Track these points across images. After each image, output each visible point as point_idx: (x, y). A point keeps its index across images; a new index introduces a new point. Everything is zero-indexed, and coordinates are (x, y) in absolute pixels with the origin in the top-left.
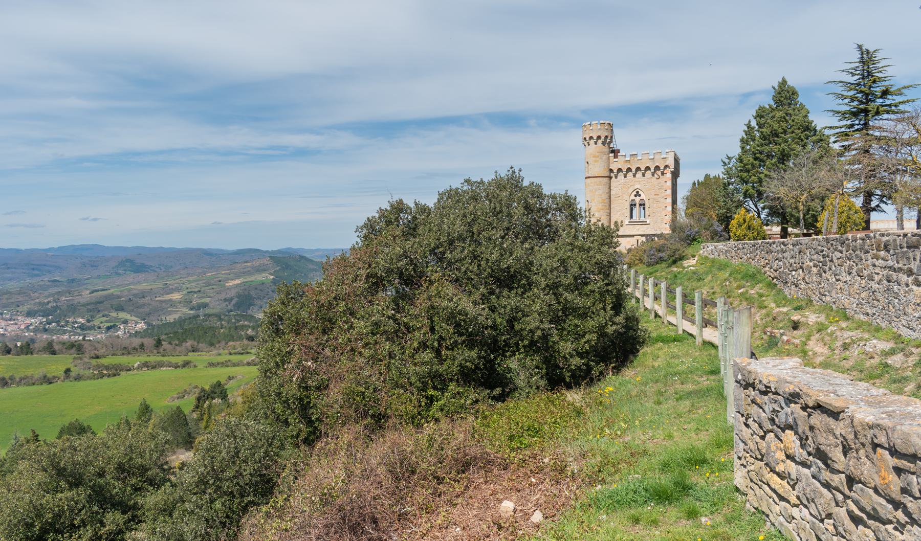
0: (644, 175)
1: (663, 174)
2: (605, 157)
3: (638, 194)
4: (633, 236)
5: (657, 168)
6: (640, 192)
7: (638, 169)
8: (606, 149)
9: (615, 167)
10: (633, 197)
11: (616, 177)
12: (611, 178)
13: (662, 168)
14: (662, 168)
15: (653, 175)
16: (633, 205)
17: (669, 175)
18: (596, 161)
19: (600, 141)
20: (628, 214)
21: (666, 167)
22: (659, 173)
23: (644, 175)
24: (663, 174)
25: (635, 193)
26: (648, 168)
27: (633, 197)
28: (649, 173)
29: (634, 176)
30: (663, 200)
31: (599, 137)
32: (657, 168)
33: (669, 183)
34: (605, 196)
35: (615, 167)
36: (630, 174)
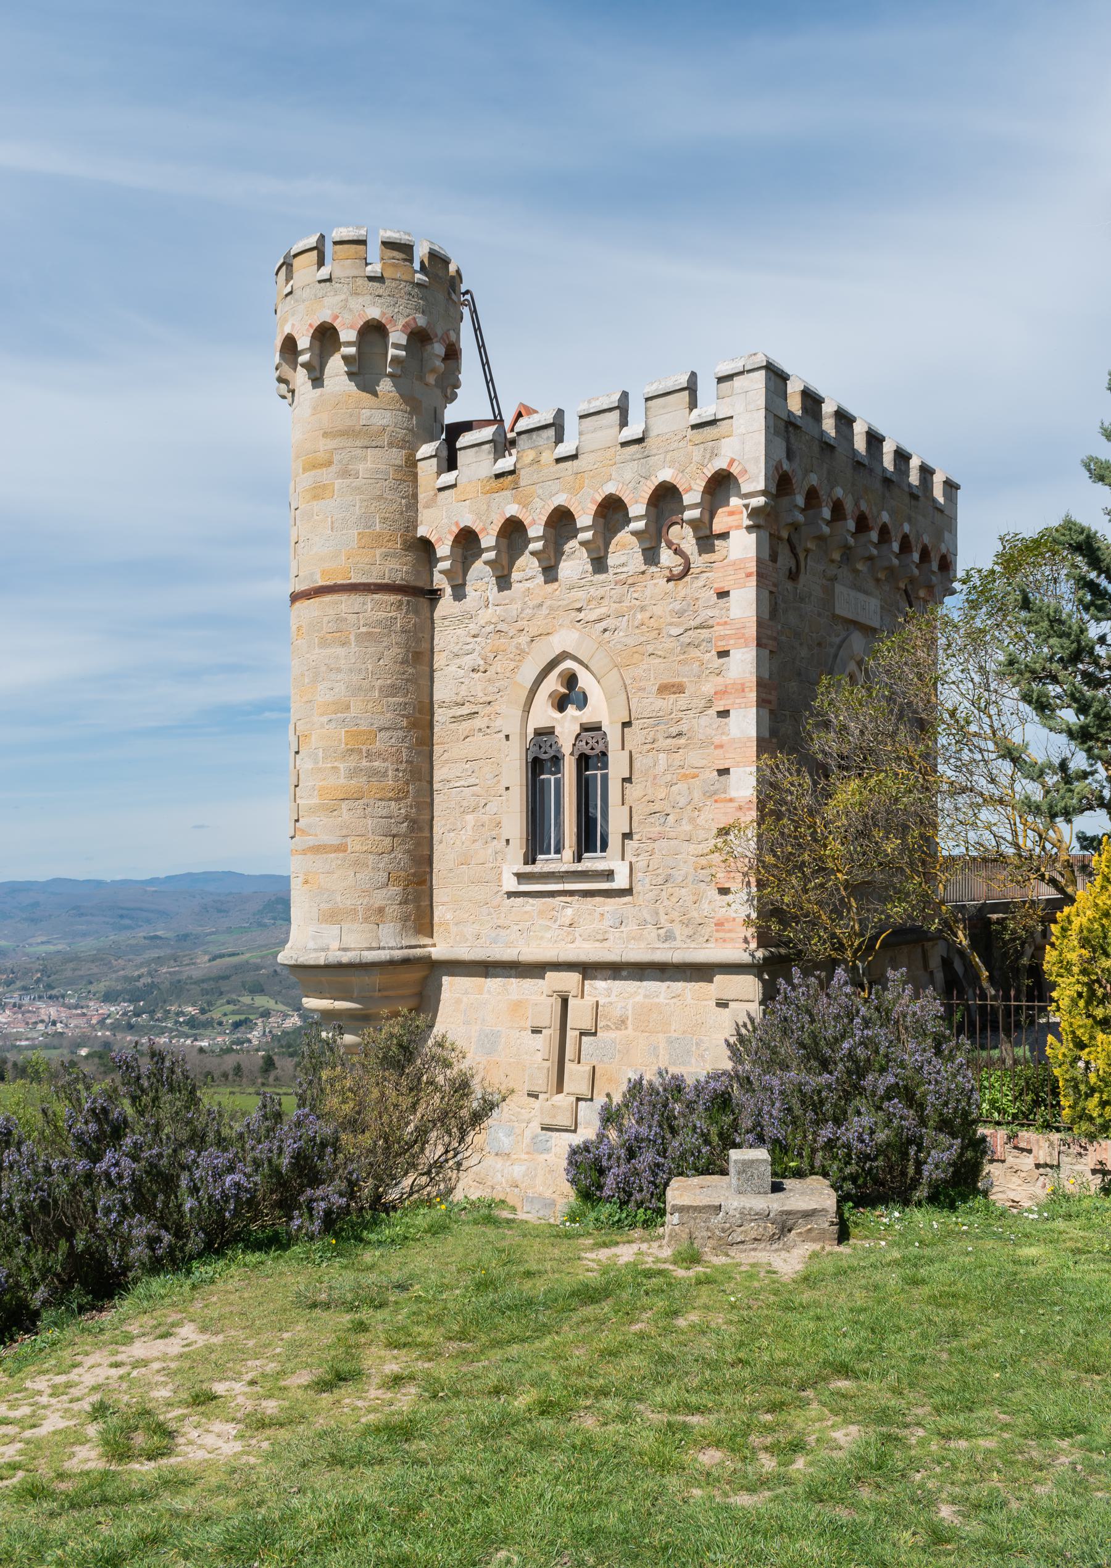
0: (599, 564)
1: (707, 540)
2: (375, 464)
3: (569, 696)
4: (536, 969)
5: (665, 498)
6: (585, 681)
7: (561, 522)
8: (383, 410)
9: (438, 525)
10: (543, 714)
11: (459, 593)
12: (434, 595)
13: (692, 496)
14: (692, 496)
15: (651, 556)
16: (540, 763)
17: (742, 546)
18: (319, 492)
19: (335, 366)
20: (515, 825)
21: (721, 485)
22: (683, 536)
23: (599, 564)
24: (707, 540)
25: (553, 684)
26: (612, 511)
27: (543, 714)
28: (625, 550)
29: (550, 572)
30: (708, 722)
31: (326, 335)
32: (665, 498)
33: (744, 605)
34: (372, 711)
35: (438, 525)
36: (527, 566)
